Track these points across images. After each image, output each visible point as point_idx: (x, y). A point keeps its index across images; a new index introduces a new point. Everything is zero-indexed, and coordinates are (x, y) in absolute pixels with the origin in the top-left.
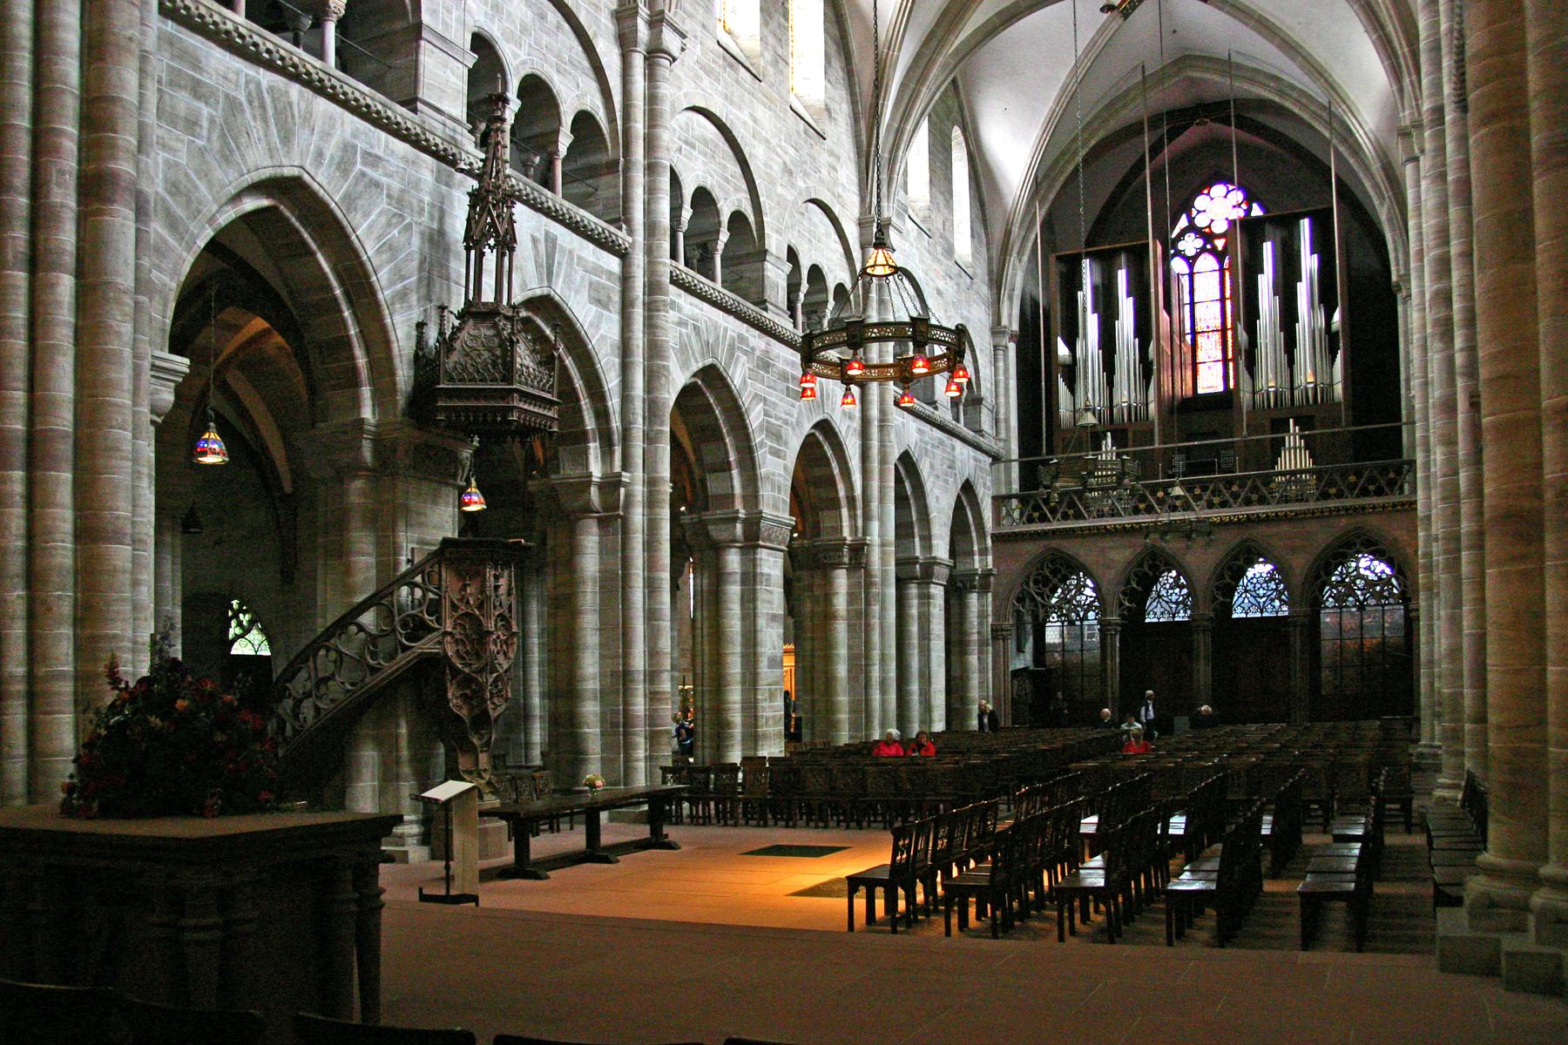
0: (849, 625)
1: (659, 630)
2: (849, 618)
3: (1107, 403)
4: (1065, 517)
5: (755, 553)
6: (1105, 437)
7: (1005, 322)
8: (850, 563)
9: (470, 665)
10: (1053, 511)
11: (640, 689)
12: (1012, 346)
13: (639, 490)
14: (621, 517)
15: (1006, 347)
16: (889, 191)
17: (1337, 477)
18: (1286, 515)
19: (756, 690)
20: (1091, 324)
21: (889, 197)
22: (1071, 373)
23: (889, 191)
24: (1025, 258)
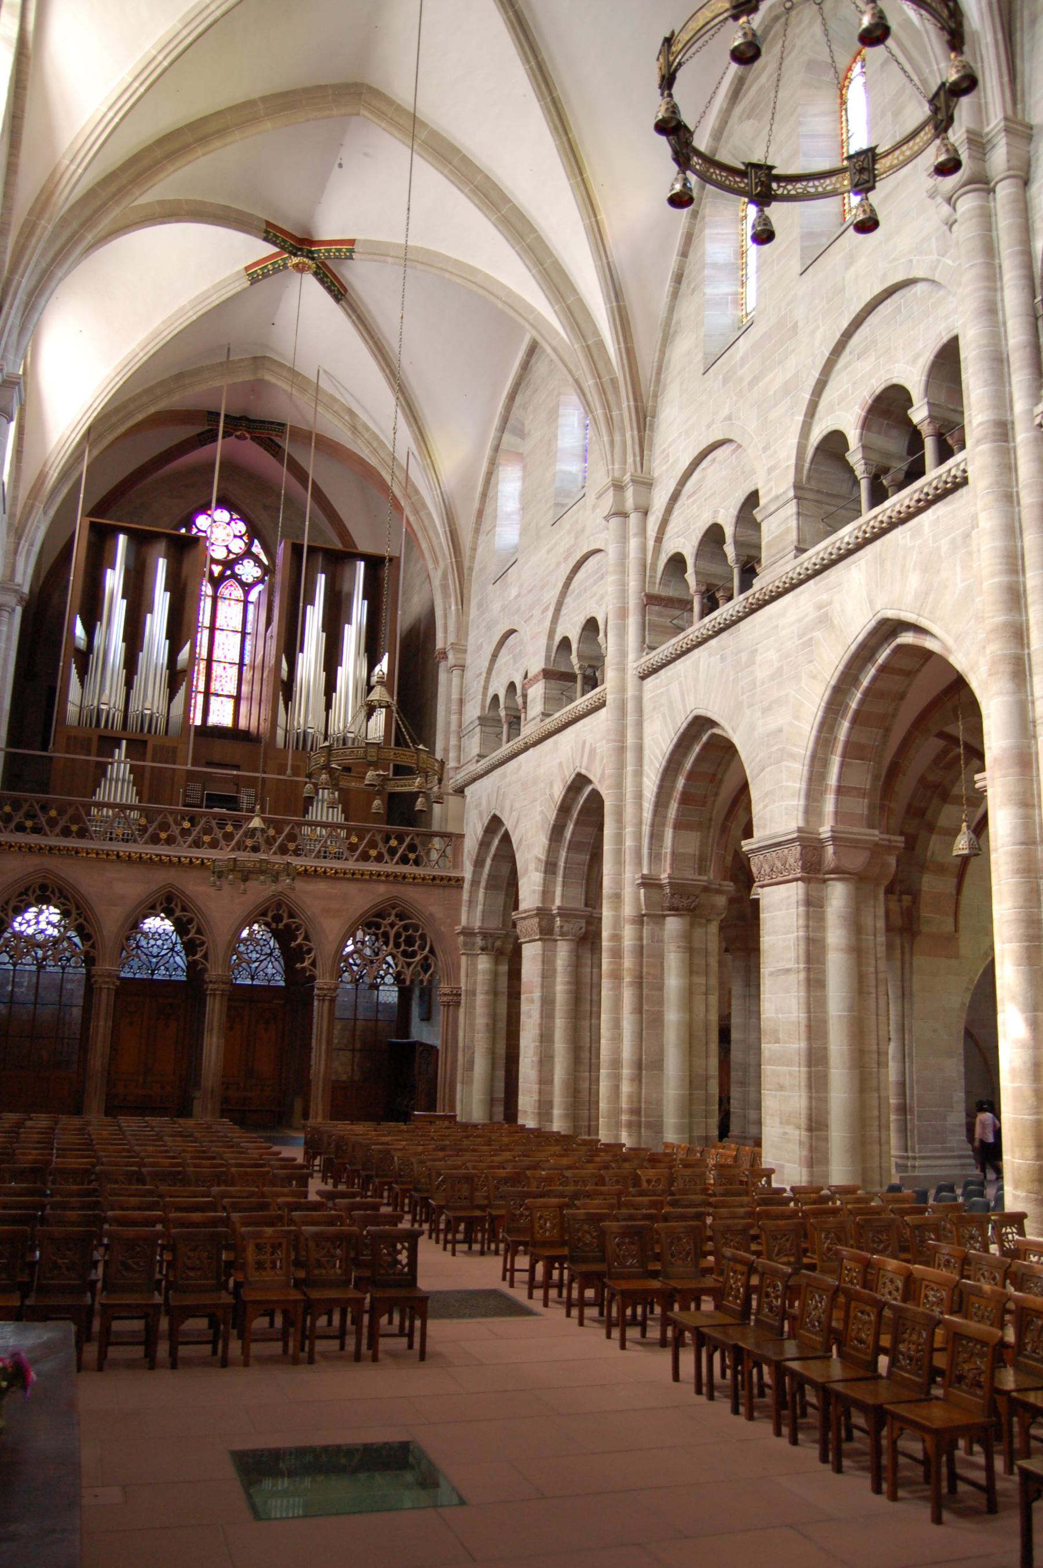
3: (122, 707)
4: (66, 833)
6: (119, 747)
7: (18, 579)
10: (52, 823)
12: (19, 610)
15: (13, 610)
16: (18, 343)
17: (378, 838)
18: (325, 872)
20: (118, 610)
21: (17, 349)
22: (84, 658)
23: (18, 343)
24: (52, 513)
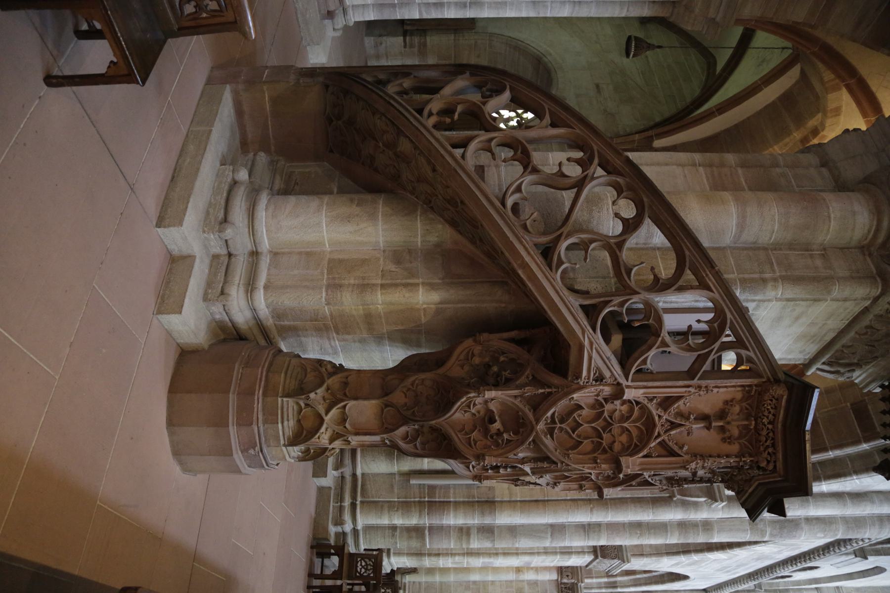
0: (511, 581)
1: (540, 537)
2: (517, 581)
5: (589, 552)
8: (562, 583)
9: (551, 432)
11: (474, 520)
13: (702, 515)
14: (671, 497)
19: (463, 554)
